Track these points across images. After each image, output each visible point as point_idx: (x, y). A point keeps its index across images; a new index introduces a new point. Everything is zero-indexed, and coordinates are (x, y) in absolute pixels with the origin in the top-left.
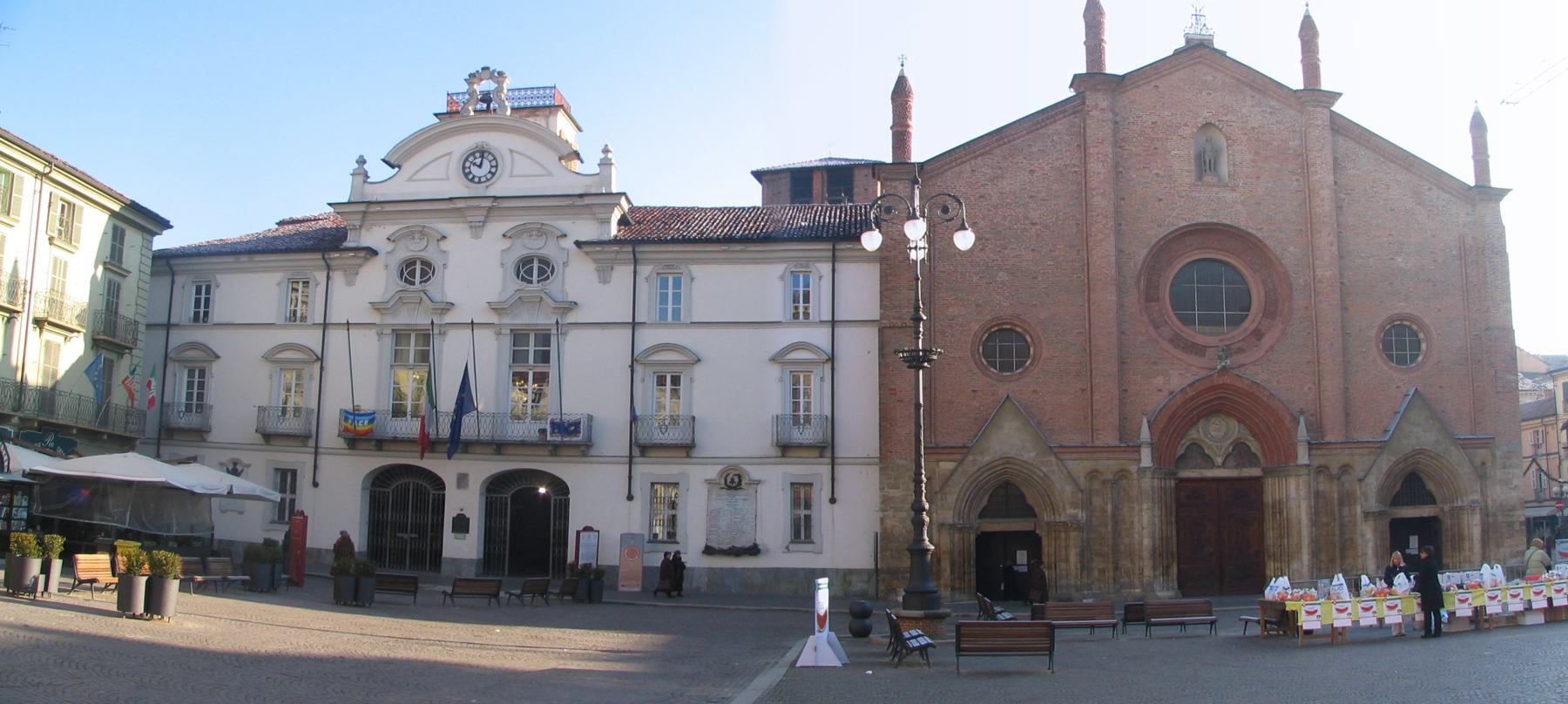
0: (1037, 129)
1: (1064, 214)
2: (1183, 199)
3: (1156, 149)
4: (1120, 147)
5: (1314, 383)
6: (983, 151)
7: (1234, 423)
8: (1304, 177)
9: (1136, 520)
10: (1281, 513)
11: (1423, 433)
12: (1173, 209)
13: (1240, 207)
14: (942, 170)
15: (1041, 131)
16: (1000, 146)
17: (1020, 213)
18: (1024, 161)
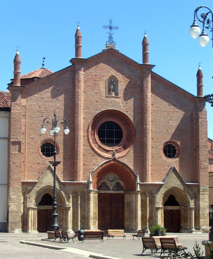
0: (60, 76)
1: (67, 105)
2: (103, 101)
3: (96, 84)
4: (85, 83)
5: (142, 164)
7: (116, 175)
8: (141, 94)
9: (86, 207)
10: (130, 205)
11: (176, 182)
12: (100, 105)
13: (121, 104)
15: (61, 76)
17: (53, 104)
18: (55, 87)
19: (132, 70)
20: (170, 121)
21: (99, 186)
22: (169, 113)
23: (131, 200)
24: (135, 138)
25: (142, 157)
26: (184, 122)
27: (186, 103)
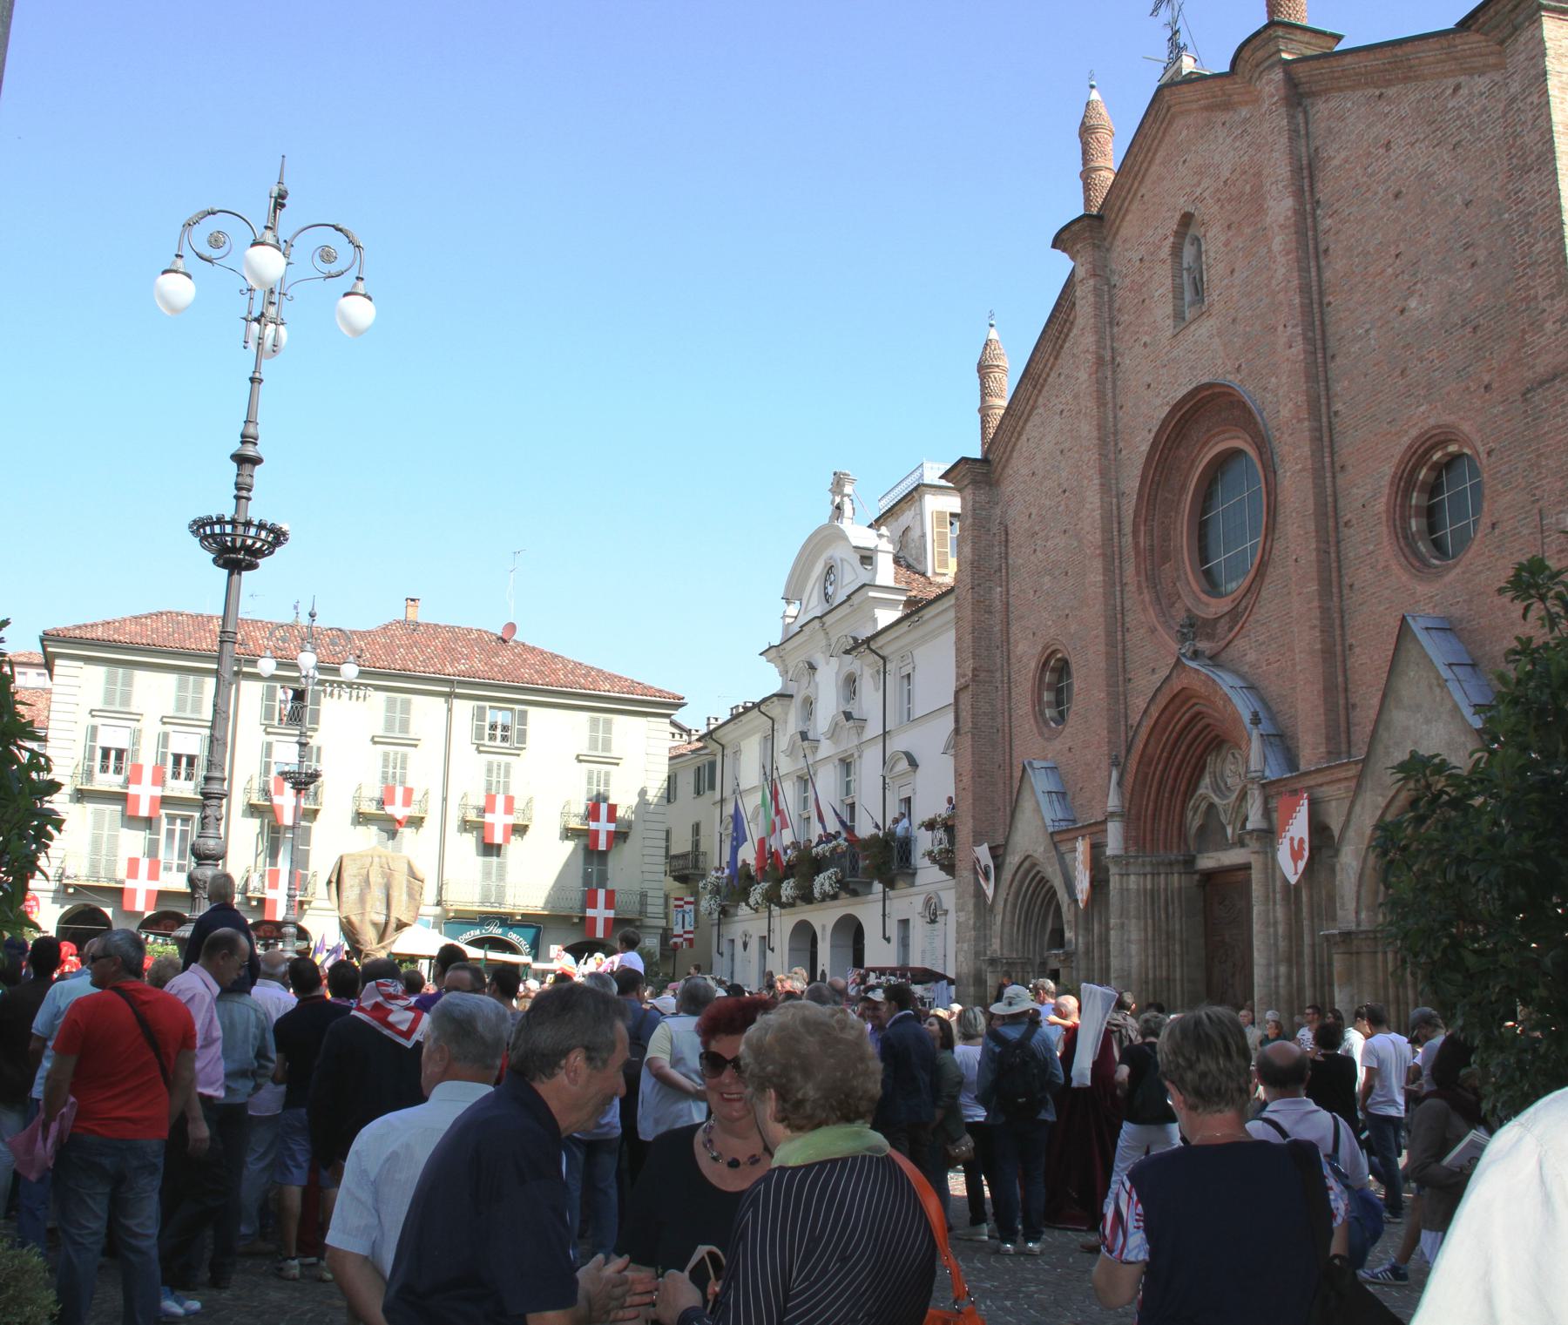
0: (1061, 347)
6: (1028, 408)
13: (1217, 340)
14: (1008, 453)
16: (1040, 391)
19: (1246, 120)
20: (1412, 294)
21: (1193, 831)
22: (1402, 247)
26: (1481, 259)
27: (1479, 114)
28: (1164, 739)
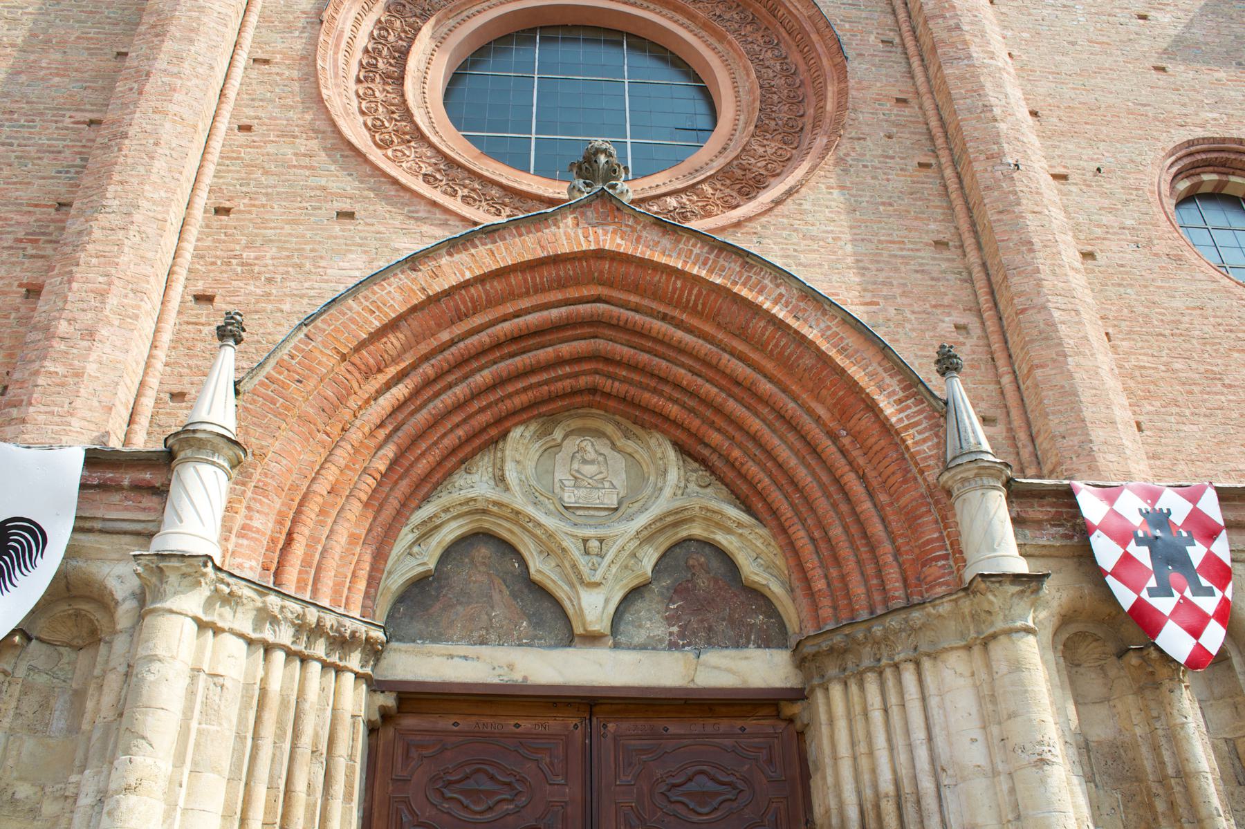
23: (922, 754)
24: (843, 93)
25: (969, 241)
28: (445, 336)
